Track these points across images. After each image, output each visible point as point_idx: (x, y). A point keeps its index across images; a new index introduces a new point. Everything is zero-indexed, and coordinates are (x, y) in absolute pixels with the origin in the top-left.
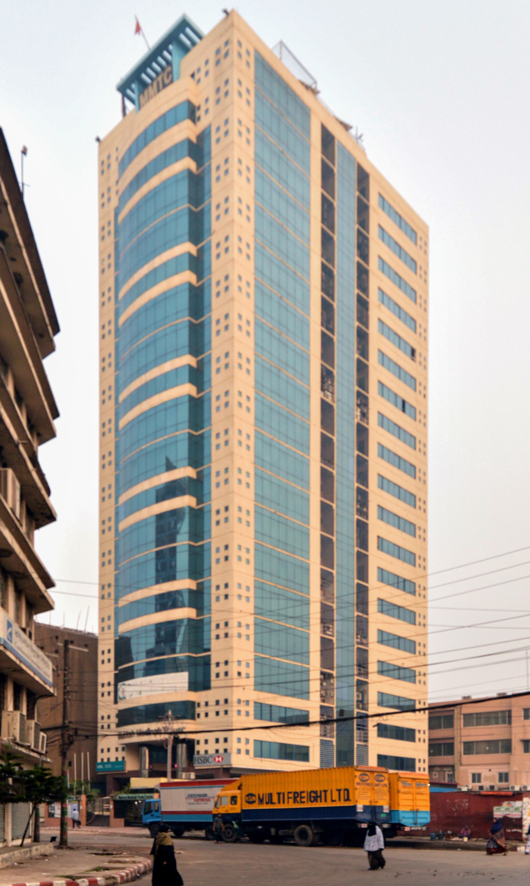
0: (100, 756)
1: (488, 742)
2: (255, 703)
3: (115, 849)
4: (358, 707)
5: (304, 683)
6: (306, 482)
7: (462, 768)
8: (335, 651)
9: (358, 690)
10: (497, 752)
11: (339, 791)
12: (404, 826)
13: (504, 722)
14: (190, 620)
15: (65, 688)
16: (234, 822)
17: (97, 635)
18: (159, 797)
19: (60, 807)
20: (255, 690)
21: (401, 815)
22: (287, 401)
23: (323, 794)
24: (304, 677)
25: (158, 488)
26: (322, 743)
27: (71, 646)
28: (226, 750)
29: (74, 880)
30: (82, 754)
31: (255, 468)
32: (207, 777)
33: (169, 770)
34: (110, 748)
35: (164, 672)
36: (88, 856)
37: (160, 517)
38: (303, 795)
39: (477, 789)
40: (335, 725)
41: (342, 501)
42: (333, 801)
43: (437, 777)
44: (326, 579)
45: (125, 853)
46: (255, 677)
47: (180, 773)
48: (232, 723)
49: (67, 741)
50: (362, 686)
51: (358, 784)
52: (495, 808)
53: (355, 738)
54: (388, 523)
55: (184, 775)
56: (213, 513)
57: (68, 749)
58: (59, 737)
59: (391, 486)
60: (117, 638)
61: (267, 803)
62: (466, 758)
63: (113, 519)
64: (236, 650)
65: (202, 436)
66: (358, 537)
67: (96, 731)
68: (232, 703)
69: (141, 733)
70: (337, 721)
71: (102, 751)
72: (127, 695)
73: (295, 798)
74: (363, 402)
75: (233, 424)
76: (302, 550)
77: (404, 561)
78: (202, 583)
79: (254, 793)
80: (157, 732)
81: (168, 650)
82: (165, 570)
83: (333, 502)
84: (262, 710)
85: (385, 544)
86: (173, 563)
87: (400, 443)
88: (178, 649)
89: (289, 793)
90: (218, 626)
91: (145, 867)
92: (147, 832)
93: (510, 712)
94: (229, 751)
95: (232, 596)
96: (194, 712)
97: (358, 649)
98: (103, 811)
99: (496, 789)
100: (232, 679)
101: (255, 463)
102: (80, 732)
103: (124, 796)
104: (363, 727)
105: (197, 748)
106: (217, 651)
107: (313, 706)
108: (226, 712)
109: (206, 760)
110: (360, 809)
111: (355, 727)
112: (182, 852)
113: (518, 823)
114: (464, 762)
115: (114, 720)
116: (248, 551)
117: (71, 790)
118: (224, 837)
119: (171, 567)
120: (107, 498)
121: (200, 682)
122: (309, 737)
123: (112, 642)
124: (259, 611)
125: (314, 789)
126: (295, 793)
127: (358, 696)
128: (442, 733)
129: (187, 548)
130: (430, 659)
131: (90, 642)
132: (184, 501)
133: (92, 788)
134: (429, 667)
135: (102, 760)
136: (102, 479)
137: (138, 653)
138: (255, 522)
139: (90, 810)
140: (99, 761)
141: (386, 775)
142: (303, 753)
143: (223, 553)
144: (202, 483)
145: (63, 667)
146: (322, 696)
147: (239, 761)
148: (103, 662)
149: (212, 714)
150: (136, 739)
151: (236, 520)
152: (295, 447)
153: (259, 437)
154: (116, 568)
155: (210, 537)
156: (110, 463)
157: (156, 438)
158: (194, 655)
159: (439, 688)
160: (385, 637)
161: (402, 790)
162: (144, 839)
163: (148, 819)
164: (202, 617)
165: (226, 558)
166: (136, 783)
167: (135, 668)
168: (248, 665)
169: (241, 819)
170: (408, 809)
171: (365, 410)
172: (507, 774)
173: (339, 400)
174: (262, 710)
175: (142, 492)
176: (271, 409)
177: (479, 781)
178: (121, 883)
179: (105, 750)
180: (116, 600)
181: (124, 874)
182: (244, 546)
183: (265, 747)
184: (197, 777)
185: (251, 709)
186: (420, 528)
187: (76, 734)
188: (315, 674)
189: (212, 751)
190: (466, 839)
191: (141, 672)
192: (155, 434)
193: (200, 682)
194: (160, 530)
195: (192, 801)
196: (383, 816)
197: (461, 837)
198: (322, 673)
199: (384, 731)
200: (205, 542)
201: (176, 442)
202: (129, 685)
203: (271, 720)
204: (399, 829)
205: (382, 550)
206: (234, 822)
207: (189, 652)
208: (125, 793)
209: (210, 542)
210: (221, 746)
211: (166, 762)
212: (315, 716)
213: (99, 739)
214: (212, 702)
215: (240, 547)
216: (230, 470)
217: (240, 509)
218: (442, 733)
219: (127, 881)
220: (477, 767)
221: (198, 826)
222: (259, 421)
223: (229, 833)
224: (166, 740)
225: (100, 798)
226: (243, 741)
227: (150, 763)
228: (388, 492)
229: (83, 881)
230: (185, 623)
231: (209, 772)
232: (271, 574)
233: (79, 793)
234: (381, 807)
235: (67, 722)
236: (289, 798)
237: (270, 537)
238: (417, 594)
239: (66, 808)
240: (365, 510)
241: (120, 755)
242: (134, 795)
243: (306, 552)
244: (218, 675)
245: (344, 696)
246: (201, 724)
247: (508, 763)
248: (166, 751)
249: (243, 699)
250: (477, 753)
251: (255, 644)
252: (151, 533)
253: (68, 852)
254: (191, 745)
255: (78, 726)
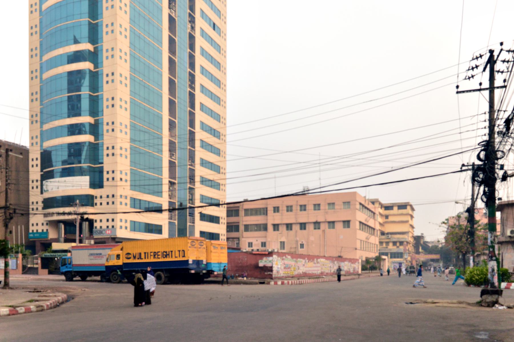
0: (31, 228)
1: (256, 225)
2: (131, 198)
3: (42, 289)
4: (189, 203)
5: (159, 186)
6: (160, 64)
7: (243, 239)
8: (177, 168)
9: (189, 192)
10: (260, 230)
11: (179, 251)
12: (214, 271)
13: (264, 214)
14: (90, 143)
15: (7, 181)
16: (118, 271)
17: (28, 148)
18: (71, 255)
19: (4, 261)
20: (131, 190)
21: (213, 265)
22: (149, 11)
23: (170, 253)
24: (160, 183)
25: (69, 54)
26: (170, 223)
27: (10, 153)
28: (113, 227)
29: (14, 308)
30: (19, 227)
31: (130, 50)
32: (101, 242)
33: (77, 238)
34: (38, 223)
35: (74, 176)
36: (24, 293)
37: (70, 73)
38: (159, 254)
39: (251, 251)
40: (177, 212)
41: (181, 79)
42: (176, 257)
43: (231, 244)
44: (172, 125)
45: (49, 291)
46: (131, 181)
47: (84, 240)
48: (117, 209)
49: (8, 217)
50: (192, 190)
51: (190, 247)
52: (260, 261)
53: (188, 221)
54: (206, 95)
55: (87, 241)
56: (105, 76)
57: (9, 222)
58: (3, 214)
59: (208, 73)
60: (42, 151)
61: (138, 259)
62: (246, 234)
63: (39, 71)
64: (119, 164)
65: (97, 24)
66: (190, 102)
67: (29, 211)
68: (117, 196)
69: (59, 214)
70: (178, 209)
71: (33, 225)
72: (49, 188)
73: (154, 256)
74: (192, 20)
75: (116, 20)
76: (158, 106)
77: (214, 119)
78: (98, 120)
79: (130, 252)
80: (69, 214)
81: (76, 161)
82: (74, 109)
83: (175, 119)
84: (135, 203)
85: (204, 108)
86: (79, 105)
87: (212, 48)
88: (83, 161)
89: (151, 252)
90: (108, 148)
91: (63, 299)
92: (63, 277)
93: (267, 208)
94: (115, 227)
95: (117, 171)
96: (93, 201)
97: (190, 168)
98: (33, 264)
99: (260, 250)
100: (117, 181)
101: (130, 47)
102: (17, 211)
103: (48, 254)
104: (192, 215)
105: (95, 224)
106: (107, 164)
107: (164, 202)
108: (113, 203)
109: (101, 232)
110: (190, 262)
111: (188, 214)
112: (86, 289)
113: (271, 269)
114: (244, 236)
115: (41, 205)
116: (126, 174)
117: (12, 248)
118: (112, 280)
119: (77, 108)
120: (34, 78)
121: (97, 183)
122: (162, 219)
123: (39, 152)
124: (132, 140)
125: (165, 250)
126: (154, 252)
127: (189, 196)
128: (233, 219)
129: (88, 96)
130: (228, 176)
131: (24, 152)
132: (86, 65)
133: (26, 249)
134: (227, 180)
135: (33, 231)
136: (31, 43)
137: (56, 162)
138: (130, 84)
139: (25, 264)
140: (31, 231)
141: (204, 242)
142: (158, 229)
143: (110, 102)
144: (97, 55)
145: (5, 167)
146: (169, 195)
147: (121, 234)
148: (33, 166)
149: (105, 203)
150: (56, 218)
151: (119, 82)
152: (153, 41)
153: (132, 31)
154: (41, 104)
155: (103, 91)
156: (36, 32)
157: (67, 21)
158: (93, 166)
159: (232, 194)
160: (204, 162)
161: (213, 250)
162: (61, 282)
163: (64, 269)
164: (97, 70)
165: (113, 106)
166: (55, 246)
167: (55, 171)
168: (126, 174)
169: (122, 269)
170: (216, 262)
171: (193, 25)
172: (265, 243)
173: (179, 16)
174: (135, 203)
175: (58, 55)
176: (140, 14)
177: (252, 247)
178: (47, 309)
179: (35, 225)
180: (41, 57)
181: (49, 304)
182: (124, 147)
183: (137, 225)
184: (95, 243)
185: (128, 201)
186: (222, 100)
187: (15, 212)
188: (166, 180)
189: (104, 227)
190: (245, 278)
191: (59, 174)
192: (67, 18)
193: (97, 183)
194: (70, 83)
195: (92, 257)
196: (203, 266)
197: (243, 277)
198: (170, 182)
199: (204, 217)
200: (99, 45)
201: (81, 25)
202: (51, 182)
203: (140, 209)
204: (211, 273)
205: (203, 111)
206: (118, 271)
207: (90, 163)
208: (49, 252)
209: (102, 45)
210: (110, 224)
211: (75, 233)
212: (165, 206)
213: (31, 216)
214: (104, 196)
215: (121, 100)
216: (115, 49)
217: (121, 75)
218: (233, 219)
219: (51, 308)
220: (251, 239)
221: (96, 273)
222: (132, 21)
223: (115, 277)
224: (76, 219)
225: (32, 256)
226: (124, 221)
227: (65, 234)
228: (206, 77)
229: (21, 309)
230: (87, 144)
231: (103, 240)
232: (140, 119)
233: (17, 252)
234: (202, 261)
235: (8, 204)
236: (151, 255)
237: (139, 95)
238: (221, 155)
239: (8, 262)
240: (193, 85)
241: (45, 228)
242: (54, 254)
243: (160, 107)
244: (108, 179)
245: (181, 196)
246: (97, 209)
247: (266, 237)
248: (75, 226)
249: (123, 194)
250: (251, 231)
251: (131, 161)
252: (64, 83)
253: (10, 291)
254: (91, 222)
255: (16, 207)
